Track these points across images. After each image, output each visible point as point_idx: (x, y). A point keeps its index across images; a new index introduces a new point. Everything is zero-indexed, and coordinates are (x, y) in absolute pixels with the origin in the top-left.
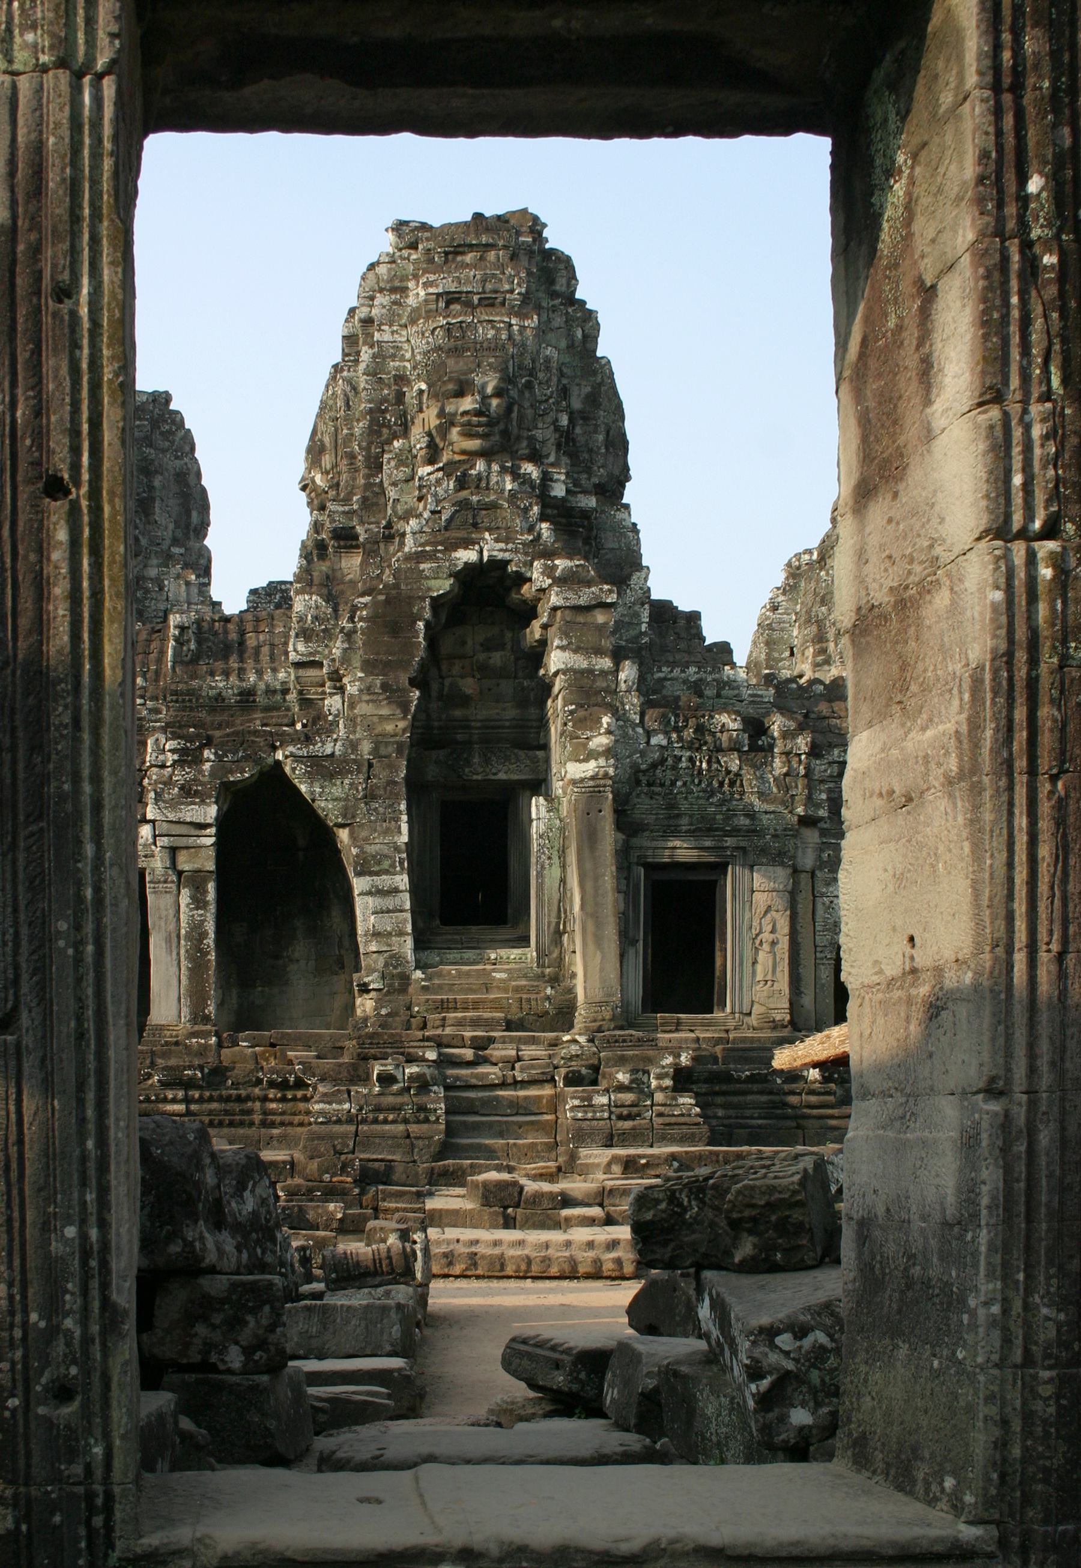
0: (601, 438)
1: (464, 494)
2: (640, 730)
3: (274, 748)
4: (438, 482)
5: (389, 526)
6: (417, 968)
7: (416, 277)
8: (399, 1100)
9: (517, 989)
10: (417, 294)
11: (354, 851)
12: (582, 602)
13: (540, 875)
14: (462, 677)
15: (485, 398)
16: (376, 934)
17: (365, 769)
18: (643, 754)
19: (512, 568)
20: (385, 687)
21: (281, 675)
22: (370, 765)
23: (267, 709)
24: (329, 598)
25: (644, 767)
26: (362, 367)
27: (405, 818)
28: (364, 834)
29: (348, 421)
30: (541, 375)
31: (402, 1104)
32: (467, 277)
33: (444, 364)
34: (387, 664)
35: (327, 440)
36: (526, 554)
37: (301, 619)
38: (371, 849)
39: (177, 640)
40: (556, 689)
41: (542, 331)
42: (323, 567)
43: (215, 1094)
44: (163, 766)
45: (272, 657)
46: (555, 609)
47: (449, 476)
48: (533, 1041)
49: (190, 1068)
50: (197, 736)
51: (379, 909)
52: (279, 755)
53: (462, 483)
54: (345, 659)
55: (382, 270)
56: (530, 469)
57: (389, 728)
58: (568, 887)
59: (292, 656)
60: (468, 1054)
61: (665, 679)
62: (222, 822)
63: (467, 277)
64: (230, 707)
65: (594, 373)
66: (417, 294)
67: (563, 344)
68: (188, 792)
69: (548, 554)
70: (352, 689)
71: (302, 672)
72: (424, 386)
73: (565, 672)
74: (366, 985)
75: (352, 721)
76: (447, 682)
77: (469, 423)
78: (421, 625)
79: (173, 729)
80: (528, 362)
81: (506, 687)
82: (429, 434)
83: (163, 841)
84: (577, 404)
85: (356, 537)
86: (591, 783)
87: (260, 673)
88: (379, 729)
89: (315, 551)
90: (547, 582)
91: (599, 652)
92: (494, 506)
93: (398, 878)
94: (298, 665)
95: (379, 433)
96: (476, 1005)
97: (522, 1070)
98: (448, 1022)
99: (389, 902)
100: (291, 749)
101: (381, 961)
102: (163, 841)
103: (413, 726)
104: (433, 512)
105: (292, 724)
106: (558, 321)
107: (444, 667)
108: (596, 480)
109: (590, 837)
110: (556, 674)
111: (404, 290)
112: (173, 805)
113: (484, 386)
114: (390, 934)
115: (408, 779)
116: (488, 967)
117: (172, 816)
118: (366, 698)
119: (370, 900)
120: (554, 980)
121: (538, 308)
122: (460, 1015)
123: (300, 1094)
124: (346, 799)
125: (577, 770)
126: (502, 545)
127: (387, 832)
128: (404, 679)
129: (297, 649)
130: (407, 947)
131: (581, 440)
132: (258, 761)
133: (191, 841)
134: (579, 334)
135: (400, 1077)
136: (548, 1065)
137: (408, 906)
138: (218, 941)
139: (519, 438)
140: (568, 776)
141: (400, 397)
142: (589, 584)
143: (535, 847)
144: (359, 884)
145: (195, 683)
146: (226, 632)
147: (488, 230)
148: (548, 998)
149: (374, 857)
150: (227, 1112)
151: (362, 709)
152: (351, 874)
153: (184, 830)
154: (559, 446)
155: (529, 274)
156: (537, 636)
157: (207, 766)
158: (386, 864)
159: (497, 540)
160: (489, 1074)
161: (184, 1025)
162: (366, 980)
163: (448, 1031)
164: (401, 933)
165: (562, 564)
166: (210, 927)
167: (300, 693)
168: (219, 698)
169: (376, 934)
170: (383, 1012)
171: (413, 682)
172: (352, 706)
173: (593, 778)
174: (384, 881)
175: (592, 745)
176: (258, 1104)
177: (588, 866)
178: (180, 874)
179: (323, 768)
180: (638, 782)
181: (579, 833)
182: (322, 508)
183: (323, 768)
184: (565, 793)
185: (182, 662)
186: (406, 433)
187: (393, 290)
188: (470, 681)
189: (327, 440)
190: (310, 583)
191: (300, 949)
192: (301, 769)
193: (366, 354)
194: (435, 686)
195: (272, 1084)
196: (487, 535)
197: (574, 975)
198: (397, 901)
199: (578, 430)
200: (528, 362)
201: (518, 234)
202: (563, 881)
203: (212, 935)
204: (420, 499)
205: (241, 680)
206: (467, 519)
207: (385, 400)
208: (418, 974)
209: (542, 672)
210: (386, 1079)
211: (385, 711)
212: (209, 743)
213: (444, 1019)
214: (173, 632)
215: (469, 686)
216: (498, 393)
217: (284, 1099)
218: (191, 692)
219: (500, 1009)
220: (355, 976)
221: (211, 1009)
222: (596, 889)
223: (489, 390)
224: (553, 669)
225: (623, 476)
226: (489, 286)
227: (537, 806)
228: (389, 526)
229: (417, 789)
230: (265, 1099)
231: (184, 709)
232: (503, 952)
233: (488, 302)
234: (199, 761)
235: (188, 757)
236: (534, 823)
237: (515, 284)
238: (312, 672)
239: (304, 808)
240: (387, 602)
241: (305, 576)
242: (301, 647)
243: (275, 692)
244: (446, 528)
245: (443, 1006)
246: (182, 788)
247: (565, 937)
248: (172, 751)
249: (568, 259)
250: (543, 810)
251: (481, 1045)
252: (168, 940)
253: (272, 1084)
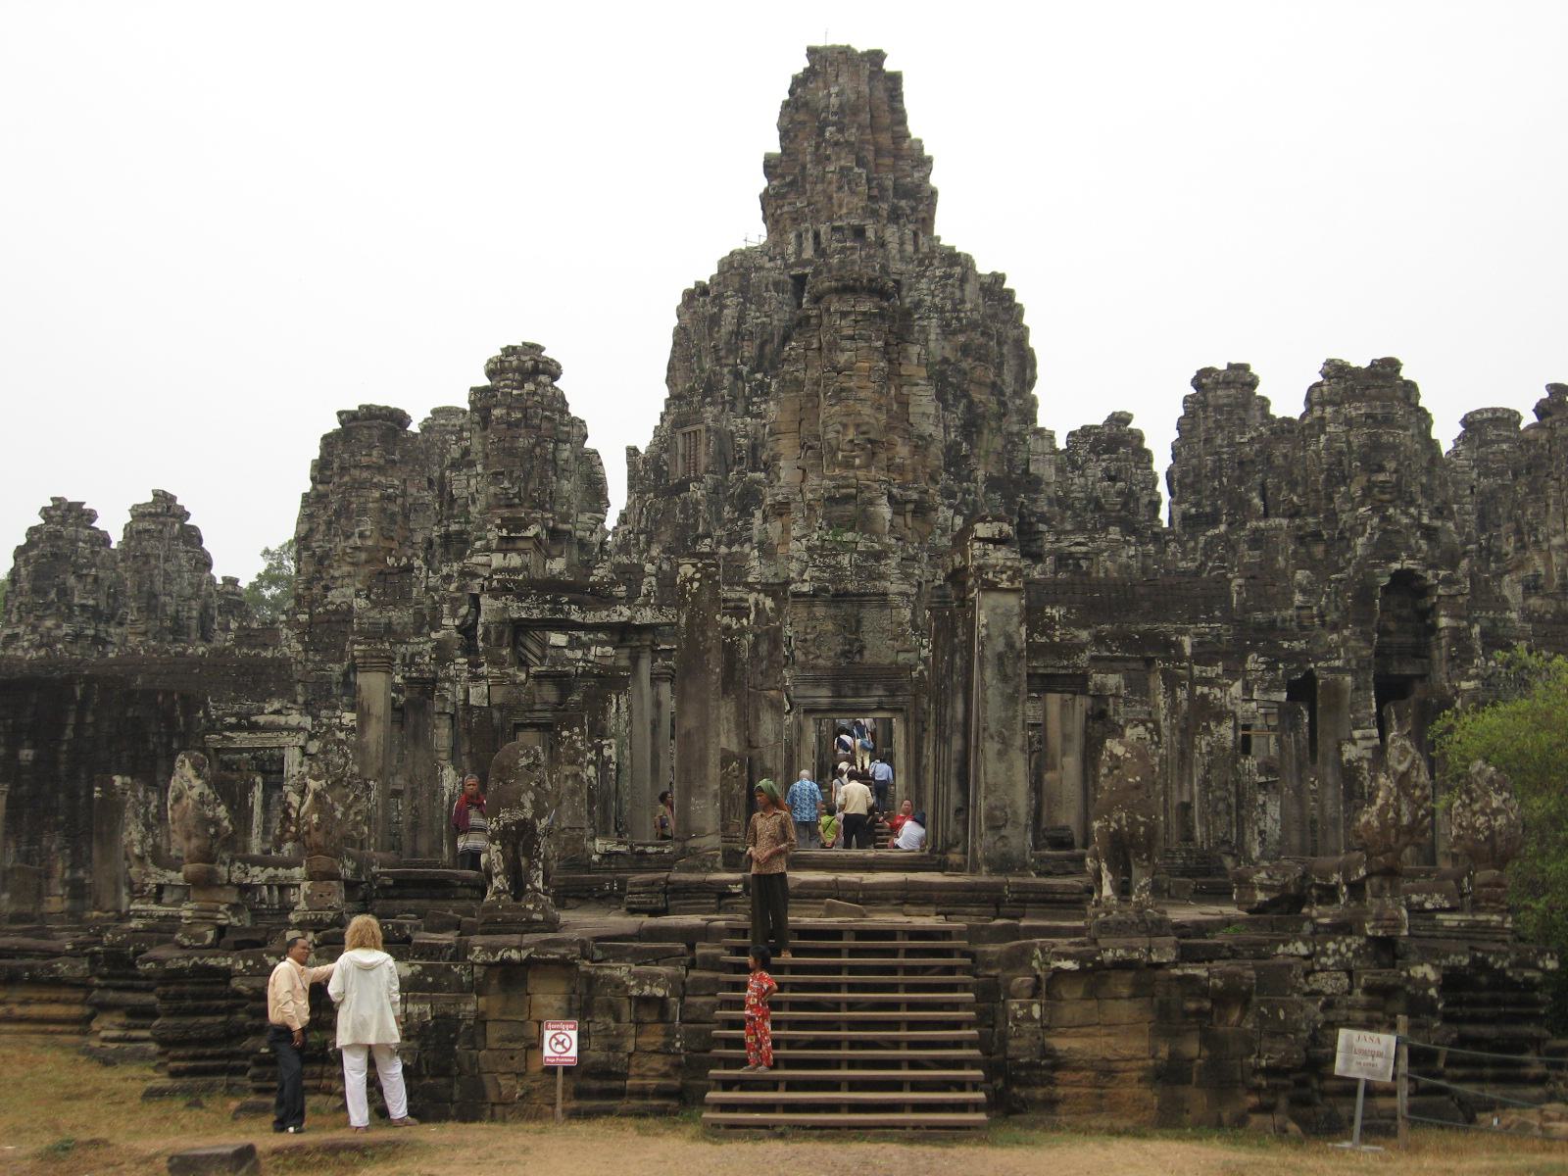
92: (1398, 532)
102: (1262, 711)
151: (1352, 643)
174: (1367, 732)
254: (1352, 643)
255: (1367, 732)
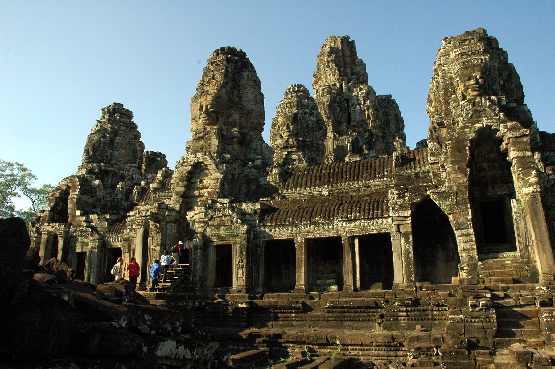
0: (514, 86)
1: (475, 107)
2: (545, 174)
3: (427, 191)
4: (467, 105)
5: (453, 120)
6: (479, 261)
7: (452, 50)
8: (479, 313)
9: (515, 267)
10: (453, 55)
11: (455, 222)
12: (518, 135)
13: (517, 226)
14: (482, 162)
15: (477, 80)
16: (465, 250)
17: (455, 195)
18: (548, 182)
19: (493, 128)
20: (459, 168)
21: (427, 167)
22: (457, 193)
23: (424, 178)
24: (439, 143)
25: (549, 186)
26: (440, 77)
27: (470, 210)
28: (457, 216)
29: (438, 92)
30: (493, 71)
31: (480, 315)
32: (467, 48)
33: (463, 72)
34: (459, 161)
35: (432, 98)
36: (497, 123)
37: (431, 150)
38: (460, 221)
39: (396, 160)
40: (513, 164)
41: (491, 58)
42: (435, 134)
43: (416, 309)
44: (394, 199)
45: (423, 161)
46: (509, 138)
47: (470, 103)
48: (524, 288)
49: (407, 299)
50: (403, 189)
51: (465, 242)
52: (428, 193)
53: (474, 105)
54: (445, 161)
55: (442, 51)
56: (494, 98)
57: (462, 181)
58: (528, 229)
59: (430, 161)
60: (501, 294)
61: (549, 156)
62: (412, 215)
63: (467, 48)
64: (413, 178)
65: (509, 68)
66: (453, 55)
67: (498, 61)
68: (402, 207)
69: (504, 122)
70: (449, 170)
71: (433, 166)
72: (458, 79)
73: (516, 158)
74: (462, 268)
75: (449, 180)
76: (478, 165)
77: (473, 87)
78: (467, 148)
79: (396, 187)
80: (488, 68)
81: (496, 164)
82: (462, 92)
83: (395, 223)
84: (505, 78)
85: (444, 124)
86: (532, 194)
87: (420, 168)
88: (458, 182)
89: (433, 130)
90: (505, 131)
91: (526, 150)
92: (484, 110)
93: (470, 230)
94: (432, 164)
95: (447, 94)
96: (501, 274)
97: (522, 300)
98: (492, 281)
99: (468, 239)
100: (432, 190)
101: (467, 260)
102: (395, 223)
103: (469, 180)
104: (466, 114)
105: (431, 182)
106: (495, 55)
107: (476, 160)
108: (514, 98)
109: (534, 214)
110: (513, 159)
111: (449, 55)
112: (398, 210)
113: (476, 77)
114: (469, 250)
115: (469, 197)
116: (503, 259)
117: (397, 215)
118: (453, 172)
119: (461, 238)
120: (528, 263)
121: (489, 53)
122: (496, 278)
123: (444, 308)
124: (450, 205)
125: (526, 190)
126: (489, 121)
127: (464, 215)
128: (464, 165)
129: (431, 159)
130: (475, 253)
131: (508, 87)
132: (422, 195)
133: (403, 222)
134: (502, 58)
135: (478, 305)
136: (532, 298)
137: (474, 239)
138: (414, 254)
139: (489, 89)
140: (524, 193)
141: (452, 83)
142: (519, 129)
143: (514, 216)
144: (457, 233)
145: (402, 172)
146: (410, 156)
147: (471, 35)
148: (527, 270)
149: (461, 223)
150: (420, 315)
151: (452, 176)
152: (454, 230)
153: (401, 219)
154: (501, 90)
155: (485, 44)
156: (505, 147)
157: (407, 198)
158: (465, 226)
159: (487, 120)
160: (510, 302)
161: (405, 284)
162: (463, 266)
163: (493, 284)
164: (473, 249)
165: (509, 124)
166: (411, 250)
167: (433, 172)
168: (409, 176)
169: (465, 250)
170: (469, 277)
171: (467, 166)
172: (449, 175)
173: (532, 193)
174: (465, 231)
175: (530, 181)
176: (430, 312)
177: (536, 223)
178: (401, 233)
179: (442, 196)
180: (548, 192)
181: (531, 212)
182: (434, 117)
183: (442, 196)
184: (522, 198)
185: (398, 166)
186: (455, 93)
187: (446, 55)
188: (485, 164)
189: (432, 98)
190: (433, 139)
191: (440, 254)
192: (435, 196)
193: (440, 73)
194: (474, 166)
195: (434, 305)
196: (484, 118)
197: (535, 262)
198: (471, 238)
199: (506, 85)
200: (488, 68)
201: (479, 34)
202: (526, 228)
203: (412, 253)
204: (462, 111)
205: (415, 170)
206: (477, 115)
207: (448, 85)
208: (480, 263)
209: (507, 158)
210: (474, 306)
211: (460, 176)
212: (407, 191)
213: (491, 279)
214: (394, 158)
215: (485, 165)
216: (481, 78)
217: (438, 310)
218: (401, 175)
219: (510, 275)
220: (459, 264)
221: (413, 278)
222: (540, 231)
223: (478, 77)
224: (512, 157)
225: (523, 96)
226: (473, 49)
227: (513, 203)
228: (453, 120)
229: (472, 200)
230: (432, 310)
231: (399, 180)
232: (508, 254)
233: (473, 54)
234: (404, 197)
235: (401, 196)
236: (513, 209)
237: (481, 47)
238: (436, 165)
239: (437, 209)
240: (456, 142)
241: (432, 138)
242: (432, 158)
243: (425, 173)
244: (471, 118)
245: (490, 275)
246: (400, 205)
247: (530, 248)
248: (396, 194)
249: (495, 38)
250: (515, 204)
251: (505, 289)
252: (399, 255)
253: (434, 305)
254: (452, 176)
255: (465, 231)
